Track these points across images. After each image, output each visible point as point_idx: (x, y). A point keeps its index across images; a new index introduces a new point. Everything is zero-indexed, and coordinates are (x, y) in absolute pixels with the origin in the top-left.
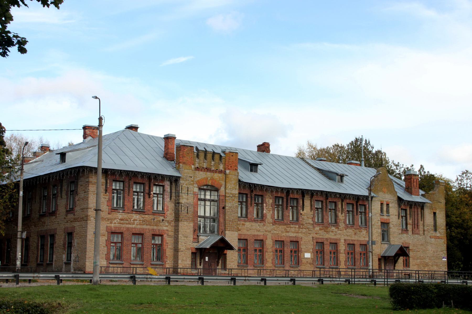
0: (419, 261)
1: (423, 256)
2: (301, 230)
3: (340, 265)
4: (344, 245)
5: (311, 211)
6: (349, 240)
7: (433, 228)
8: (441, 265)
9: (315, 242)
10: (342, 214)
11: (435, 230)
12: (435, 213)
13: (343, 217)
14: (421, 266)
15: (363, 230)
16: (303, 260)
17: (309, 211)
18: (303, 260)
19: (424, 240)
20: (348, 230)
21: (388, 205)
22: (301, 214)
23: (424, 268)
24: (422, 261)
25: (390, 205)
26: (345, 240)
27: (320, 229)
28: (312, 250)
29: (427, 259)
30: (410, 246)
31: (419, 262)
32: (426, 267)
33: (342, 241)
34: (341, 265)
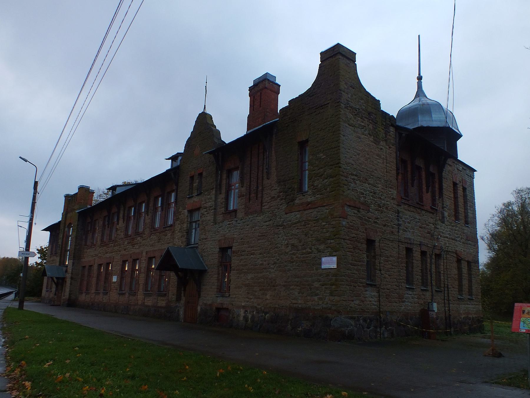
0: (250, 276)
1: (262, 264)
2: (114, 248)
3: (139, 290)
4: (145, 260)
5: (124, 223)
6: (150, 251)
9: (121, 261)
10: (148, 215)
13: (149, 219)
15: (168, 232)
16: (112, 284)
17: (123, 224)
18: (112, 284)
19: (267, 223)
20: (152, 237)
21: (201, 175)
22: (117, 229)
25: (204, 174)
26: (147, 253)
27: (128, 243)
28: (119, 271)
29: (272, 271)
30: (234, 244)
33: (144, 254)
34: (140, 290)
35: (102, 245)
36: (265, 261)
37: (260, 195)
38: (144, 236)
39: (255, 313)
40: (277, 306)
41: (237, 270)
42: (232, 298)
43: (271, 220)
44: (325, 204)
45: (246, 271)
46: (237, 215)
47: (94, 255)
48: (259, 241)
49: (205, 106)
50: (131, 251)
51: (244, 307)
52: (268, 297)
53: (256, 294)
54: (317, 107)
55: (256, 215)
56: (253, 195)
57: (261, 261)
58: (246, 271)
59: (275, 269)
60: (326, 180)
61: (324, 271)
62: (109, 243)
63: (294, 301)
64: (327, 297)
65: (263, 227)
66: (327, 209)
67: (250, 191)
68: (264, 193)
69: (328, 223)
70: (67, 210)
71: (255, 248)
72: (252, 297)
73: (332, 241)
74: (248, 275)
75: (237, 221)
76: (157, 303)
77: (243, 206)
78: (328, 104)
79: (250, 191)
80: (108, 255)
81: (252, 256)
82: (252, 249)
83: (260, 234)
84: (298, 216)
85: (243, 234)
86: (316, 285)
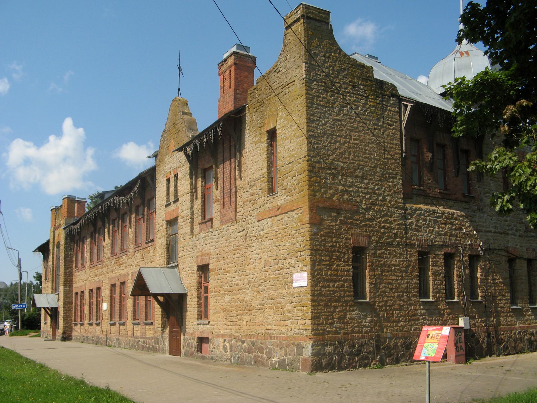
0: (227, 299)
1: (238, 284)
7: (265, 185)
8: (289, 306)
11: (271, 190)
12: (272, 134)
14: (234, 313)
20: (136, 255)
21: (176, 176)
23: (240, 320)
24: (236, 297)
25: (180, 175)
27: (115, 263)
29: (248, 291)
30: (211, 261)
31: (230, 302)
32: (246, 317)
33: (130, 275)
35: (91, 266)
36: (240, 280)
37: (233, 199)
38: (129, 254)
39: (233, 342)
40: (253, 333)
41: (214, 292)
42: (211, 325)
43: (244, 230)
44: (294, 208)
45: (223, 292)
46: (213, 224)
47: (85, 279)
48: (234, 256)
49: (179, 89)
50: (118, 272)
51: (223, 336)
52: (245, 323)
53: (234, 319)
54: (284, 86)
55: (229, 224)
56: (227, 199)
57: (237, 280)
58: (223, 292)
59: (250, 289)
60: (294, 178)
61: (296, 289)
62: (97, 264)
63: (269, 327)
64: (299, 321)
65: (237, 239)
66: (297, 214)
67: (224, 194)
68: (238, 196)
69: (298, 231)
70: (55, 226)
71: (230, 265)
72: (229, 323)
73: (302, 253)
74: (226, 297)
75: (212, 232)
76: (145, 333)
77: (219, 214)
78: (294, 81)
79: (224, 194)
80: (97, 279)
81: (228, 275)
82: (228, 266)
83: (234, 248)
84: (270, 223)
85: (218, 248)
86: (289, 306)
